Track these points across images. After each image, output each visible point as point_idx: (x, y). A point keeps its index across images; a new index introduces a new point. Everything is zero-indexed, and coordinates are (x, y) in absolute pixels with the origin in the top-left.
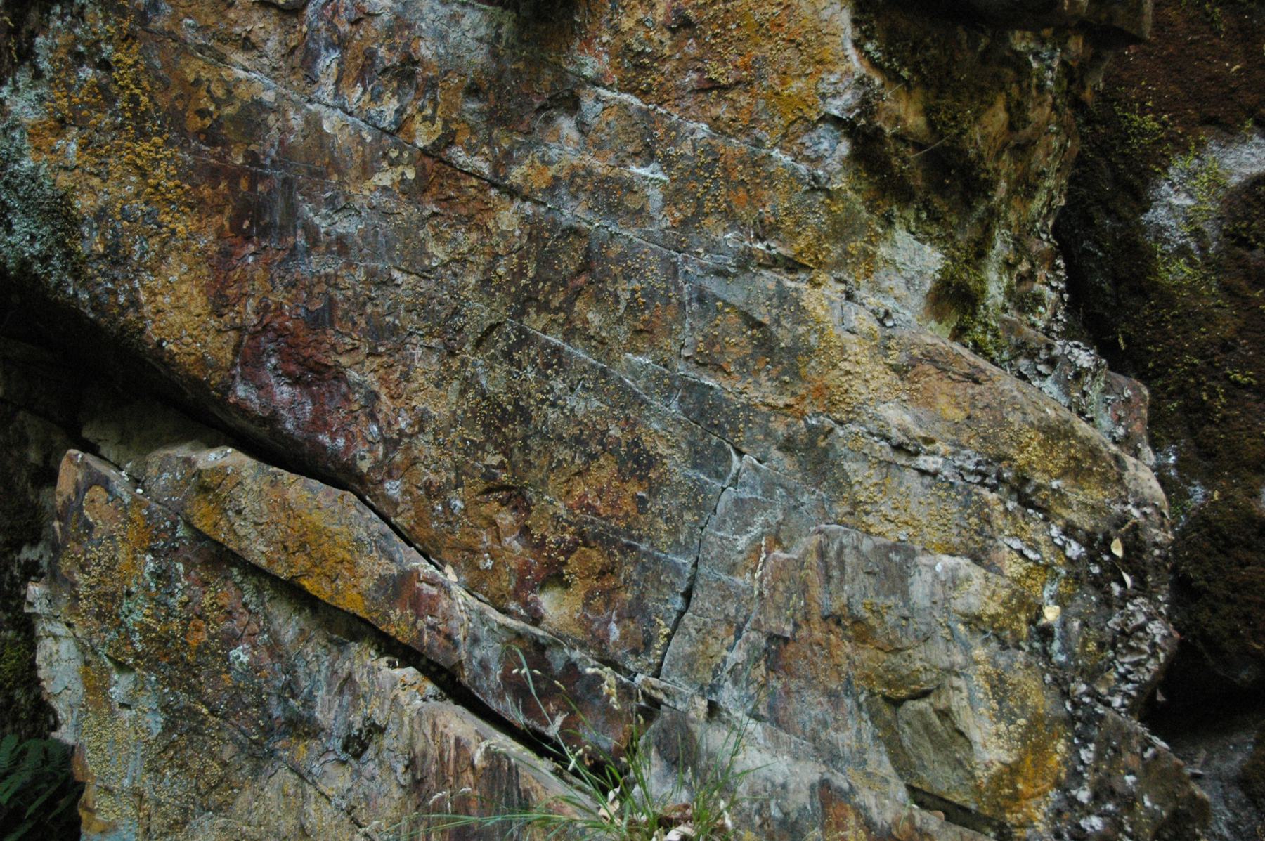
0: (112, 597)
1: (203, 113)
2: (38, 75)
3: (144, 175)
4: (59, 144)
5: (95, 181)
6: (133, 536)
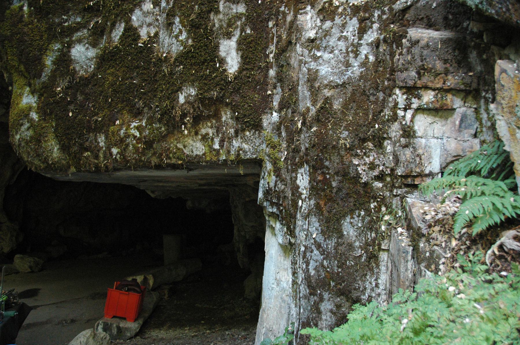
0: (512, 107)
6: (516, 87)
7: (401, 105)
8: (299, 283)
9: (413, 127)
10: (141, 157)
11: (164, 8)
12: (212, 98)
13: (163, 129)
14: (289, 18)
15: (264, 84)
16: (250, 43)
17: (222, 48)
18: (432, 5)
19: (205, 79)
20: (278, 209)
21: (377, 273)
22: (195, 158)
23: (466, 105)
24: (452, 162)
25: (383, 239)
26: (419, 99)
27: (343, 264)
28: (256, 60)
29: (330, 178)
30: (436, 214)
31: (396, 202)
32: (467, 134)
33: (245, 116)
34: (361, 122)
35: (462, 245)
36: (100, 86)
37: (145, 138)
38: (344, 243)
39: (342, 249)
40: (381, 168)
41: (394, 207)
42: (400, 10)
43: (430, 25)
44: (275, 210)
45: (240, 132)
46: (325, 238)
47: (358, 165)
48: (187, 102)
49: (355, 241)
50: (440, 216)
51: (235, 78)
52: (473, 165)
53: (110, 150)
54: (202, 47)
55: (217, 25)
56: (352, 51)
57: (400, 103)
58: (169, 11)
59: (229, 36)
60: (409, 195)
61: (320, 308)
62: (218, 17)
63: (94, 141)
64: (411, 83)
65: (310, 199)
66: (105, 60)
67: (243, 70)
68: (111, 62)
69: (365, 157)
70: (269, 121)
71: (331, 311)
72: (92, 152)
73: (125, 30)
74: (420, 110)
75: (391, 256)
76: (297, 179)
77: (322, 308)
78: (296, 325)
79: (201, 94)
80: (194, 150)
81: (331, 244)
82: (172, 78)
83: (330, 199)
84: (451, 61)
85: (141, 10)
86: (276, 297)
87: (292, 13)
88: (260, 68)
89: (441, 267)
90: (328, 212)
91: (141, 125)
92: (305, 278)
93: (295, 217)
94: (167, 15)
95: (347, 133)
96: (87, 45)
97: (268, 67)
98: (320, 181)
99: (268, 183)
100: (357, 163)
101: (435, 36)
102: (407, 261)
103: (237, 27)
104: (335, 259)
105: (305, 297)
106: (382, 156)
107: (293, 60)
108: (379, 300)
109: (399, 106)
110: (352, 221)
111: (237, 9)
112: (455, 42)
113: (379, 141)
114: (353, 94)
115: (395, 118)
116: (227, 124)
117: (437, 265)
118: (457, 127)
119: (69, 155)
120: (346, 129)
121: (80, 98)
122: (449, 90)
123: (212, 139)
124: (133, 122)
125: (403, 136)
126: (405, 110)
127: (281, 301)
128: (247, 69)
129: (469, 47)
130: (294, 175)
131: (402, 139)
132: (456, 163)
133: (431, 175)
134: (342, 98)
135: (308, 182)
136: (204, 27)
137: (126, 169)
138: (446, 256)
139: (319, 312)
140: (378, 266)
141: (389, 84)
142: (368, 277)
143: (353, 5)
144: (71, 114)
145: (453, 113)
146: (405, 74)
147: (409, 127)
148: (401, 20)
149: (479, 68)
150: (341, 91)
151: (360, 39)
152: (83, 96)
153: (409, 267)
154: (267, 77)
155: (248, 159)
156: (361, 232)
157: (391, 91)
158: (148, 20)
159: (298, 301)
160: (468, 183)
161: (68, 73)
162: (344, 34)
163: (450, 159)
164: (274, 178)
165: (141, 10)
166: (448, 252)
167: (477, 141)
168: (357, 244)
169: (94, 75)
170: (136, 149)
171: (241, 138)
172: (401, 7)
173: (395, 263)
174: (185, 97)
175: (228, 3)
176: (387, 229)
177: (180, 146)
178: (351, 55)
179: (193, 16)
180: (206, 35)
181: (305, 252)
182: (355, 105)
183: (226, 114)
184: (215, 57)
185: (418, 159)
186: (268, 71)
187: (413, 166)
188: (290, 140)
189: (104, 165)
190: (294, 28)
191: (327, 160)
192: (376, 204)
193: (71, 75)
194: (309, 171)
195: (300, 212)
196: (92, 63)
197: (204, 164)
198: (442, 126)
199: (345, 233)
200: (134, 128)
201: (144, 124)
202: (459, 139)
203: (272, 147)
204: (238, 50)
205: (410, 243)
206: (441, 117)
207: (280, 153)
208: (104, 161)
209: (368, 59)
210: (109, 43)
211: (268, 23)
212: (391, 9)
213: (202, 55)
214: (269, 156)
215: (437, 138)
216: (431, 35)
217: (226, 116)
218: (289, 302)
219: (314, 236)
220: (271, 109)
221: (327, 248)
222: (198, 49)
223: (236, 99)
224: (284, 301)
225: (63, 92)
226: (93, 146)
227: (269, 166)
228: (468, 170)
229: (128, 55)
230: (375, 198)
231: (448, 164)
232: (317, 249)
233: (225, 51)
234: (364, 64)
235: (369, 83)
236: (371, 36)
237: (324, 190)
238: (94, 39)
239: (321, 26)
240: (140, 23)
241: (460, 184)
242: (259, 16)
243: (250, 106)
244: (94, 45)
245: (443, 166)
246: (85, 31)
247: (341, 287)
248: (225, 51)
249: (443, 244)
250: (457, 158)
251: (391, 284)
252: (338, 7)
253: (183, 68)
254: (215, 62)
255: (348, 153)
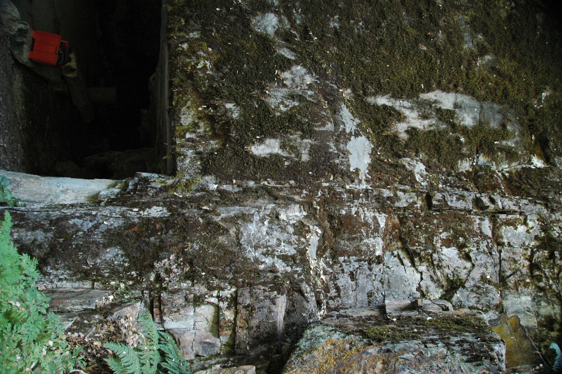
1: (344, 370)
2: (344, 337)
3: (325, 363)
4: (329, 345)
5: (321, 354)
7: (222, 293)
8: (62, 211)
9: (204, 304)
10: (179, 69)
11: (306, 93)
12: (230, 132)
13: (203, 89)
14: (297, 197)
15: (242, 177)
16: (277, 165)
17: (273, 141)
18: (305, 312)
19: (246, 126)
20: (131, 190)
21: (72, 280)
22: (178, 116)
23: (223, 346)
24: (174, 339)
25: (103, 284)
26: (227, 308)
27: (80, 249)
28: (262, 170)
29: (158, 235)
30: (125, 328)
31: (137, 293)
32: (198, 349)
33: (214, 160)
34: (207, 260)
35: (96, 350)
36: (242, 36)
37: (196, 73)
38: (99, 249)
39: (94, 248)
40: (167, 279)
41: (133, 292)
42: (301, 288)
43: (288, 313)
44: (130, 187)
45: (200, 156)
46: (103, 233)
47: (169, 259)
48: (226, 110)
49: (101, 259)
50: (124, 331)
51: (246, 152)
52: (171, 356)
53: (186, 42)
54: (273, 124)
55: (291, 137)
56: (268, 251)
57: (224, 292)
58: (304, 97)
59: (283, 147)
60: (143, 304)
61: (38, 229)
62: (298, 138)
63: (194, 28)
64: (240, 300)
65: (139, 218)
66: (264, 41)
67: (254, 159)
68: (262, 46)
69: (176, 264)
70: (210, 181)
71: (35, 240)
72: (185, 25)
73: (289, 60)
74: (218, 309)
75: (88, 291)
76: (157, 206)
77: (37, 232)
78: (23, 208)
79: (233, 123)
80: (185, 116)
81: (98, 237)
82: (248, 98)
83: (139, 236)
84: (258, 332)
85: (305, 74)
86: (50, 190)
87: (301, 200)
88: (256, 173)
89: (76, 334)
90: (127, 235)
91: (207, 70)
92: (66, 216)
93: (123, 205)
94: (301, 96)
95: (198, 249)
96: (277, 27)
97: (256, 180)
98: (155, 226)
99: (155, 181)
100: (171, 258)
101: (278, 317)
102: (81, 305)
103: (290, 154)
104: (84, 242)
105: (48, 216)
106: (178, 279)
107: (262, 201)
108: (47, 282)
109: (221, 292)
111: (304, 154)
112: (274, 333)
113: (191, 276)
114: (231, 253)
115: (211, 288)
116: (207, 145)
117: (77, 331)
118: (204, 340)
119: (182, 6)
120: (201, 248)
121: (232, 18)
122: (234, 332)
123: (194, 132)
124: (210, 63)
125: (195, 296)
126: (218, 297)
127: (47, 194)
128: (255, 162)
129: (270, 345)
130: (161, 204)
131: (192, 295)
132: (173, 341)
133: (162, 322)
134: (228, 244)
135: (155, 216)
136: (290, 126)
137: (169, 55)
138: (86, 338)
139: (34, 229)
140: (79, 280)
141: (239, 283)
142: (68, 272)
143: (307, 250)
144: (218, 9)
145: (216, 337)
146: (247, 294)
147: (203, 301)
148: (293, 289)
149: (252, 354)
150: (234, 243)
151: (278, 257)
152: (234, 21)
153: (76, 307)
154: (247, 180)
155: (176, 163)
156: (109, 264)
157: (234, 285)
158: (297, 79)
159: (46, 210)
160: (152, 352)
161: (253, 9)
162: (282, 243)
163: (176, 336)
164: (159, 186)
165: (305, 74)
166: (90, 339)
167: (193, 357)
168: (99, 261)
169: (252, 31)
170: (187, 65)
171: (195, 157)
172: (303, 288)
173: (81, 294)
174: (231, 109)
175: (310, 146)
176: (113, 287)
177: (189, 103)
178: (265, 250)
179: (299, 117)
180: (284, 127)
181: (90, 215)
182: (222, 254)
183: (216, 144)
184: (265, 135)
185: (175, 310)
186: (253, 180)
187: (169, 306)
188: (192, 200)
189: (173, 37)
190: (288, 201)
191: (174, 232)
192: (135, 275)
193: (252, 12)
194: (164, 217)
195: (128, 210)
196: (262, 31)
197: (173, 124)
198: (205, 328)
199: (108, 250)
200: (205, 64)
201: (208, 72)
202: (194, 343)
203: (186, 184)
204: (271, 155)
205: (98, 307)
206: (212, 327)
207: (181, 191)
208: (176, 36)
209: (261, 264)
210: (278, 46)
211: (293, 180)
212: (302, 281)
213: (266, 124)
214: (179, 181)
215: (194, 325)
216: (279, 314)
217: (214, 144)
218: (46, 202)
219: (105, 222)
220: (220, 183)
221: (94, 235)
222: (272, 121)
223: (229, 153)
224: (47, 197)
225: (237, 4)
226: (190, 27)
227: (170, 182)
228: (165, 351)
229: (268, 61)
230: (140, 275)
231: (172, 335)
232: (93, 226)
233: (270, 143)
234: (257, 261)
235: (241, 266)
236: (281, 266)
237: (147, 230)
238: (282, 33)
239: (290, 224)
240: (295, 72)
241: (151, 345)
242: (299, 172)
243: (223, 164)
244: (276, 33)
245: (170, 331)
246: (289, 27)
247: (58, 248)
248: (270, 143)
249: (97, 335)
250: (178, 342)
251: (61, 292)
252: (305, 237)
253: (256, 108)
254: (261, 135)
255: (180, 250)
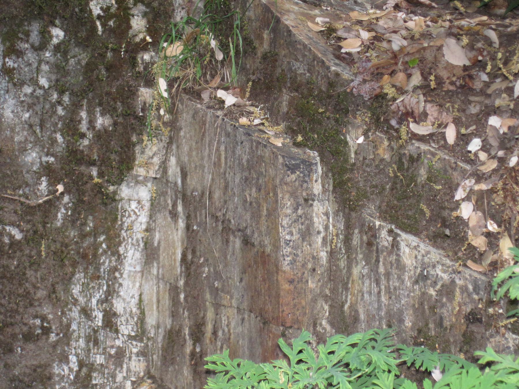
102: (308, 200)
108: (119, 378)
110: (10, 63)
140: (113, 247)
153: (318, 222)
168: (32, 157)
